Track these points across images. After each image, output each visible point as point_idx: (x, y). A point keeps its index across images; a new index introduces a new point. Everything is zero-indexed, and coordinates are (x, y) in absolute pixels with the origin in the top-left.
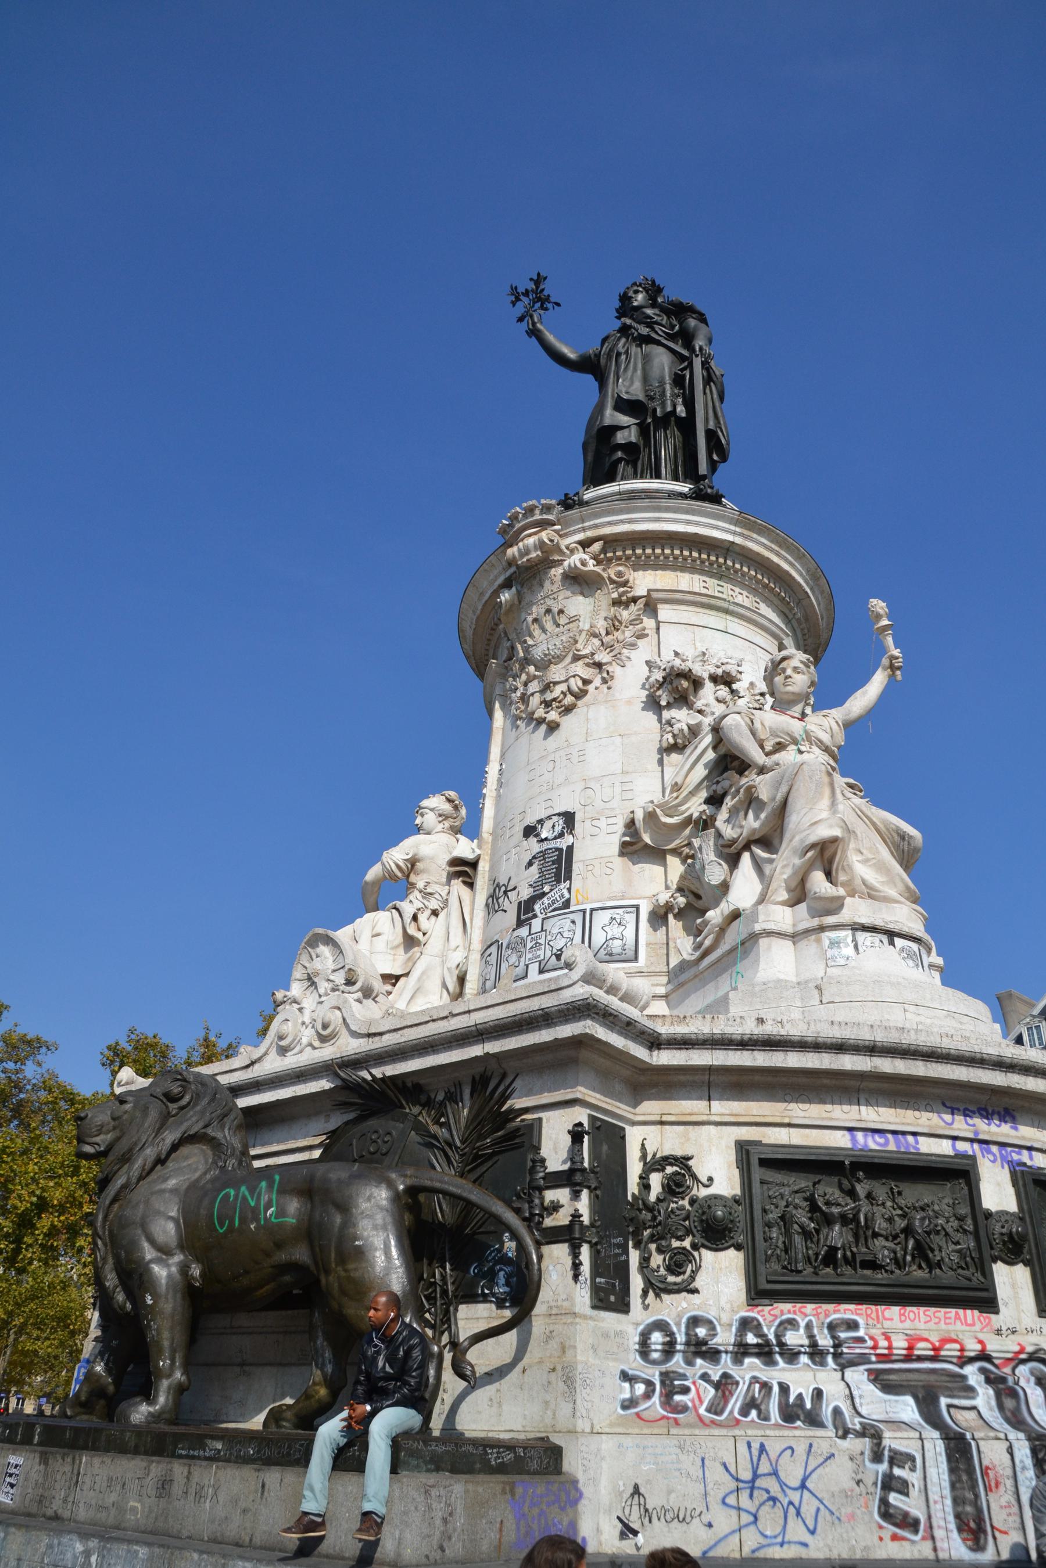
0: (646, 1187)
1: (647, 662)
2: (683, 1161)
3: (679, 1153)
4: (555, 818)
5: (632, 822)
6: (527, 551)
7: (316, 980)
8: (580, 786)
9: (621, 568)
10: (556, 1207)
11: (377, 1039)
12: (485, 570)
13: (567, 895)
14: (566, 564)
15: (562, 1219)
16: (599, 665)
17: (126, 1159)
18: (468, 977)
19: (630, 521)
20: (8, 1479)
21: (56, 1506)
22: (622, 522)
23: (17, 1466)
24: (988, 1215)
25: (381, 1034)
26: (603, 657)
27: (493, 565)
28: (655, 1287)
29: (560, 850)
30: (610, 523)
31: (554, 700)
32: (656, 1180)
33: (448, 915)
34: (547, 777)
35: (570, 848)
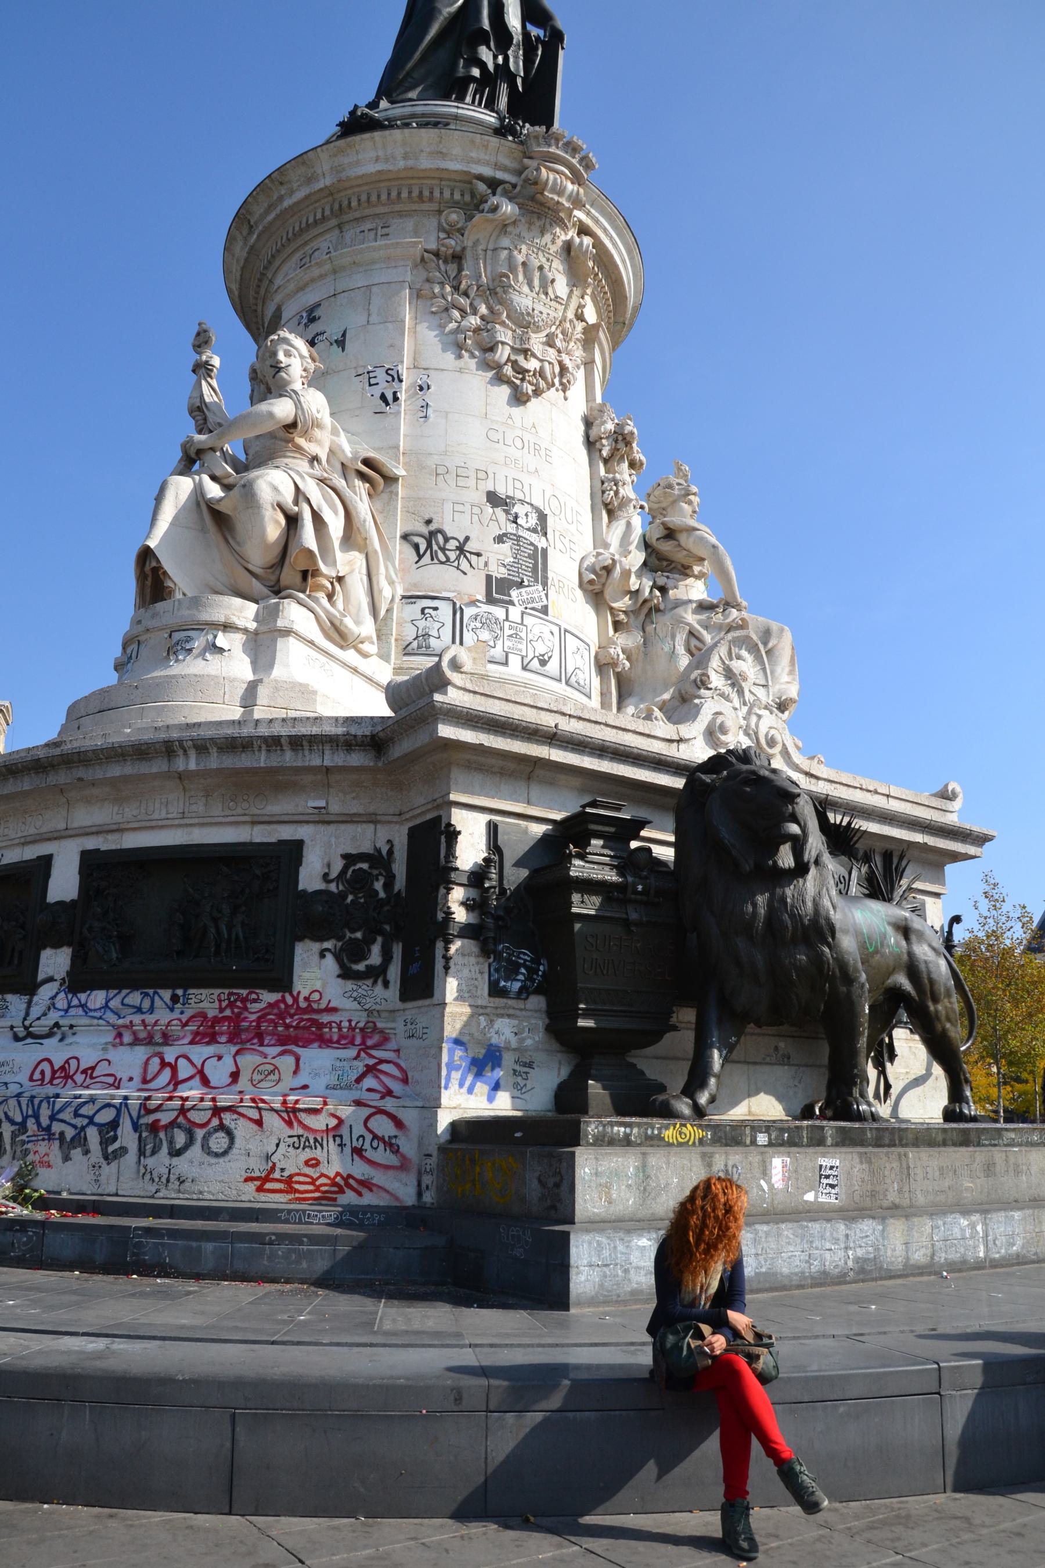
4: (528, 508)
5: (608, 570)
6: (561, 192)
7: (743, 684)
11: (813, 781)
12: (473, 142)
13: (545, 603)
16: (563, 369)
19: (615, 244)
20: (825, 1181)
21: (892, 1197)
22: (611, 238)
23: (832, 1168)
25: (817, 778)
27: (486, 147)
29: (536, 548)
30: (605, 230)
31: (528, 371)
34: (512, 452)
35: (545, 551)
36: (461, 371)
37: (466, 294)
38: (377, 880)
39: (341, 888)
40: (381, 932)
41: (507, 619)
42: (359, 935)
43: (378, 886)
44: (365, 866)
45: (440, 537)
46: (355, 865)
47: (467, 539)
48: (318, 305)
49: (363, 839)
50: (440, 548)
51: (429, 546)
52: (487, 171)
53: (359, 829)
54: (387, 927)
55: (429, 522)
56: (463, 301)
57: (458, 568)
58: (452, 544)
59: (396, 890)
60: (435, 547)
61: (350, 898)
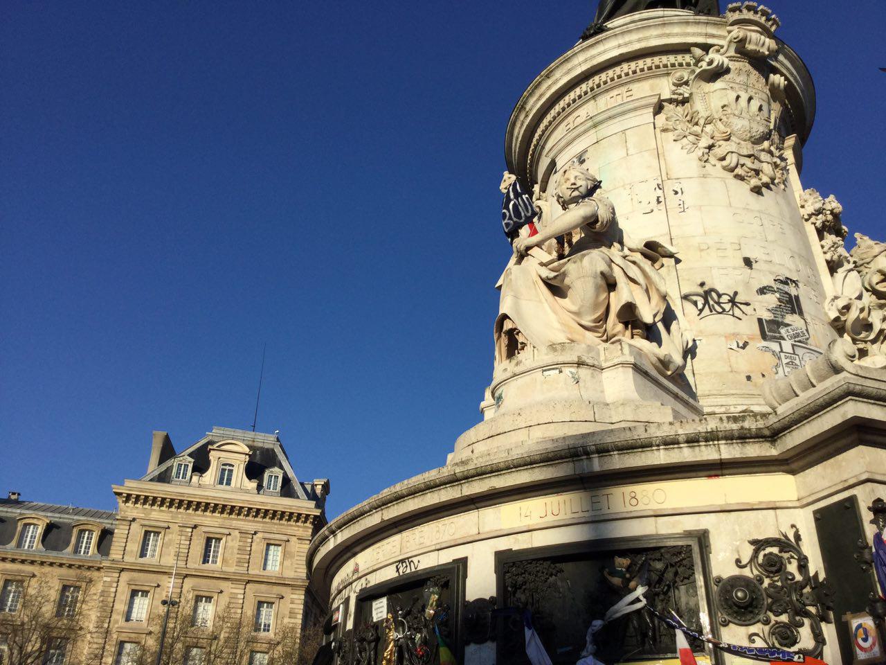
29: (790, 295)
35: (797, 298)
36: (704, 176)
37: (697, 124)
38: (790, 563)
39: (756, 572)
40: (807, 614)
41: (782, 351)
42: (784, 618)
43: (792, 568)
44: (775, 550)
45: (714, 295)
46: (764, 549)
47: (736, 293)
48: (585, 151)
49: (769, 526)
50: (716, 302)
51: (706, 302)
52: (701, 40)
53: (760, 516)
54: (812, 610)
55: (702, 284)
56: (697, 129)
57: (733, 315)
58: (725, 299)
59: (812, 574)
60: (711, 302)
61: (767, 582)
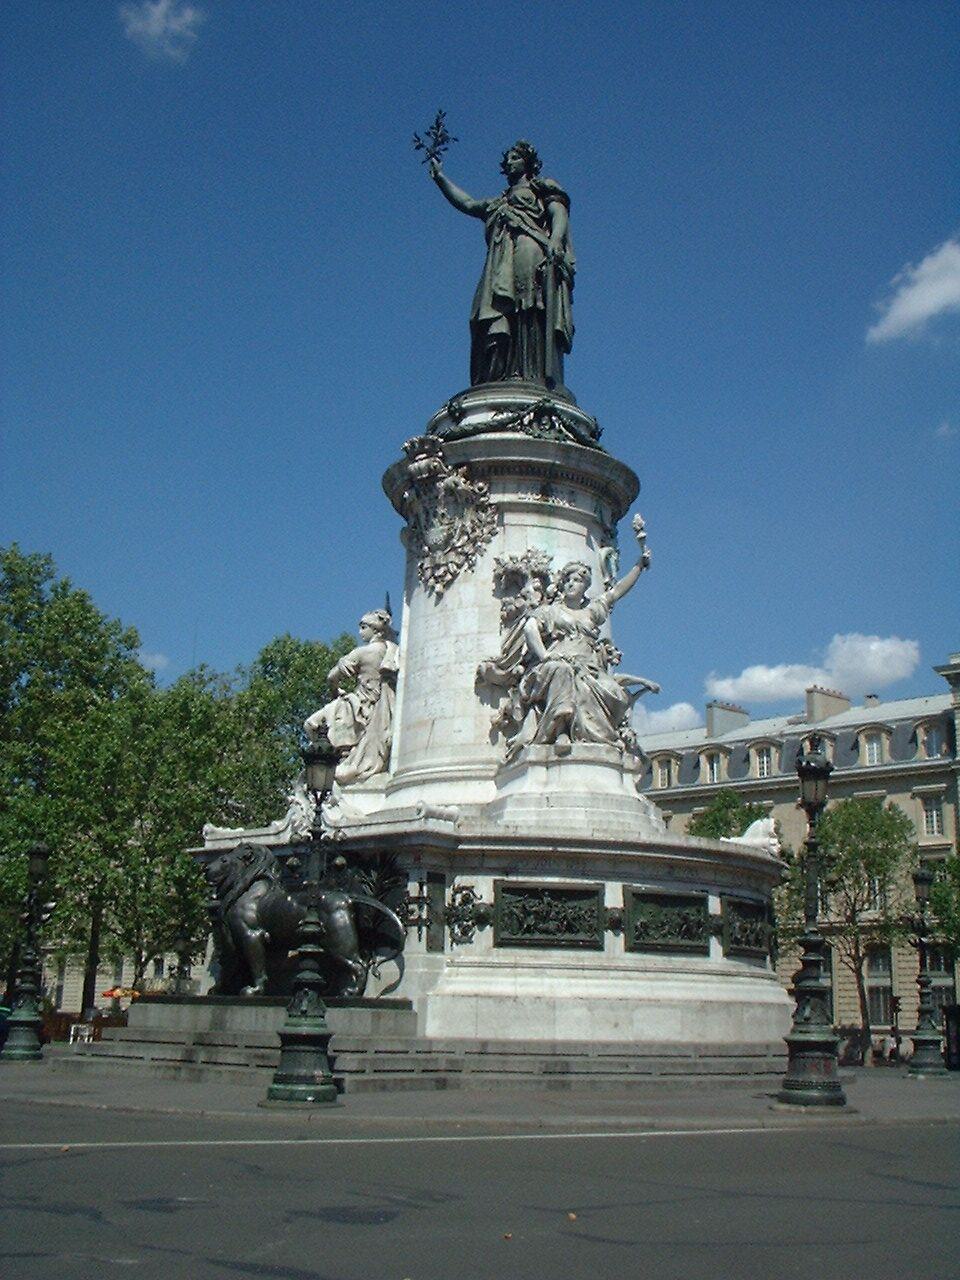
0: (454, 900)
1: (495, 559)
2: (470, 889)
3: (469, 885)
8: (454, 639)
9: (481, 484)
10: (412, 912)
14: (446, 480)
15: (414, 917)
16: (467, 555)
17: (231, 887)
18: (393, 747)
24: (606, 909)
26: (468, 549)
28: (455, 940)
32: (459, 897)
33: (380, 706)
